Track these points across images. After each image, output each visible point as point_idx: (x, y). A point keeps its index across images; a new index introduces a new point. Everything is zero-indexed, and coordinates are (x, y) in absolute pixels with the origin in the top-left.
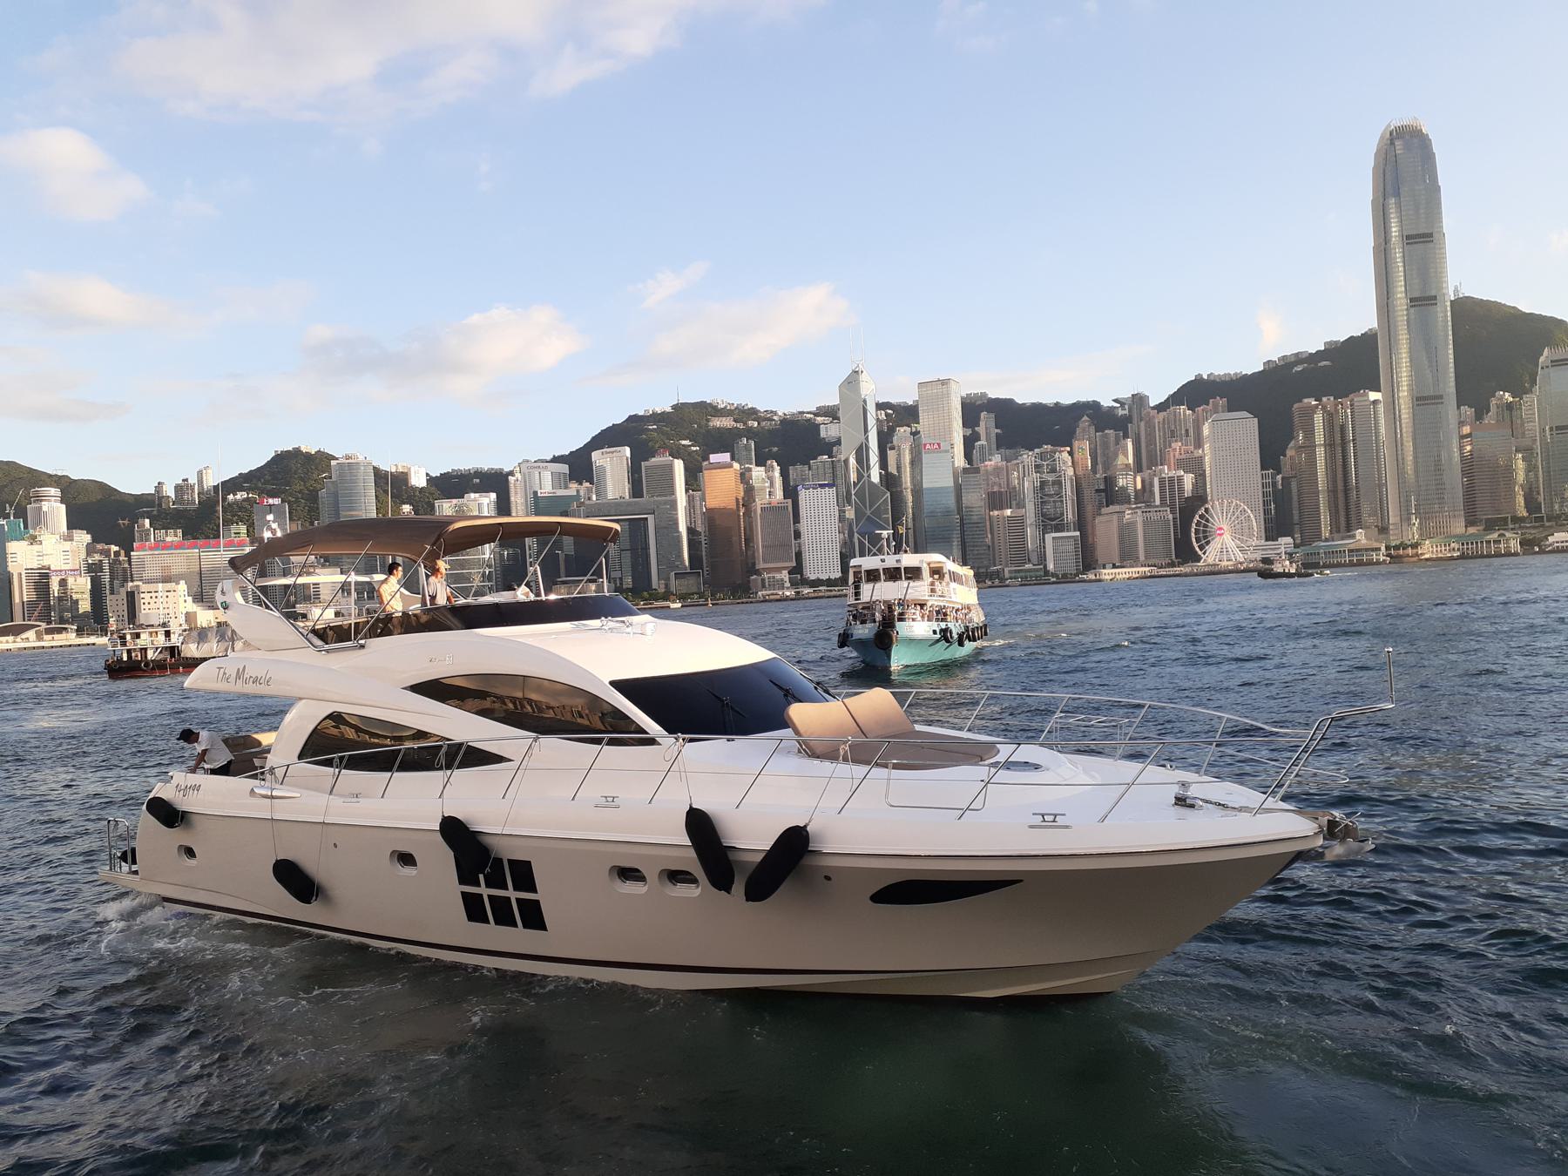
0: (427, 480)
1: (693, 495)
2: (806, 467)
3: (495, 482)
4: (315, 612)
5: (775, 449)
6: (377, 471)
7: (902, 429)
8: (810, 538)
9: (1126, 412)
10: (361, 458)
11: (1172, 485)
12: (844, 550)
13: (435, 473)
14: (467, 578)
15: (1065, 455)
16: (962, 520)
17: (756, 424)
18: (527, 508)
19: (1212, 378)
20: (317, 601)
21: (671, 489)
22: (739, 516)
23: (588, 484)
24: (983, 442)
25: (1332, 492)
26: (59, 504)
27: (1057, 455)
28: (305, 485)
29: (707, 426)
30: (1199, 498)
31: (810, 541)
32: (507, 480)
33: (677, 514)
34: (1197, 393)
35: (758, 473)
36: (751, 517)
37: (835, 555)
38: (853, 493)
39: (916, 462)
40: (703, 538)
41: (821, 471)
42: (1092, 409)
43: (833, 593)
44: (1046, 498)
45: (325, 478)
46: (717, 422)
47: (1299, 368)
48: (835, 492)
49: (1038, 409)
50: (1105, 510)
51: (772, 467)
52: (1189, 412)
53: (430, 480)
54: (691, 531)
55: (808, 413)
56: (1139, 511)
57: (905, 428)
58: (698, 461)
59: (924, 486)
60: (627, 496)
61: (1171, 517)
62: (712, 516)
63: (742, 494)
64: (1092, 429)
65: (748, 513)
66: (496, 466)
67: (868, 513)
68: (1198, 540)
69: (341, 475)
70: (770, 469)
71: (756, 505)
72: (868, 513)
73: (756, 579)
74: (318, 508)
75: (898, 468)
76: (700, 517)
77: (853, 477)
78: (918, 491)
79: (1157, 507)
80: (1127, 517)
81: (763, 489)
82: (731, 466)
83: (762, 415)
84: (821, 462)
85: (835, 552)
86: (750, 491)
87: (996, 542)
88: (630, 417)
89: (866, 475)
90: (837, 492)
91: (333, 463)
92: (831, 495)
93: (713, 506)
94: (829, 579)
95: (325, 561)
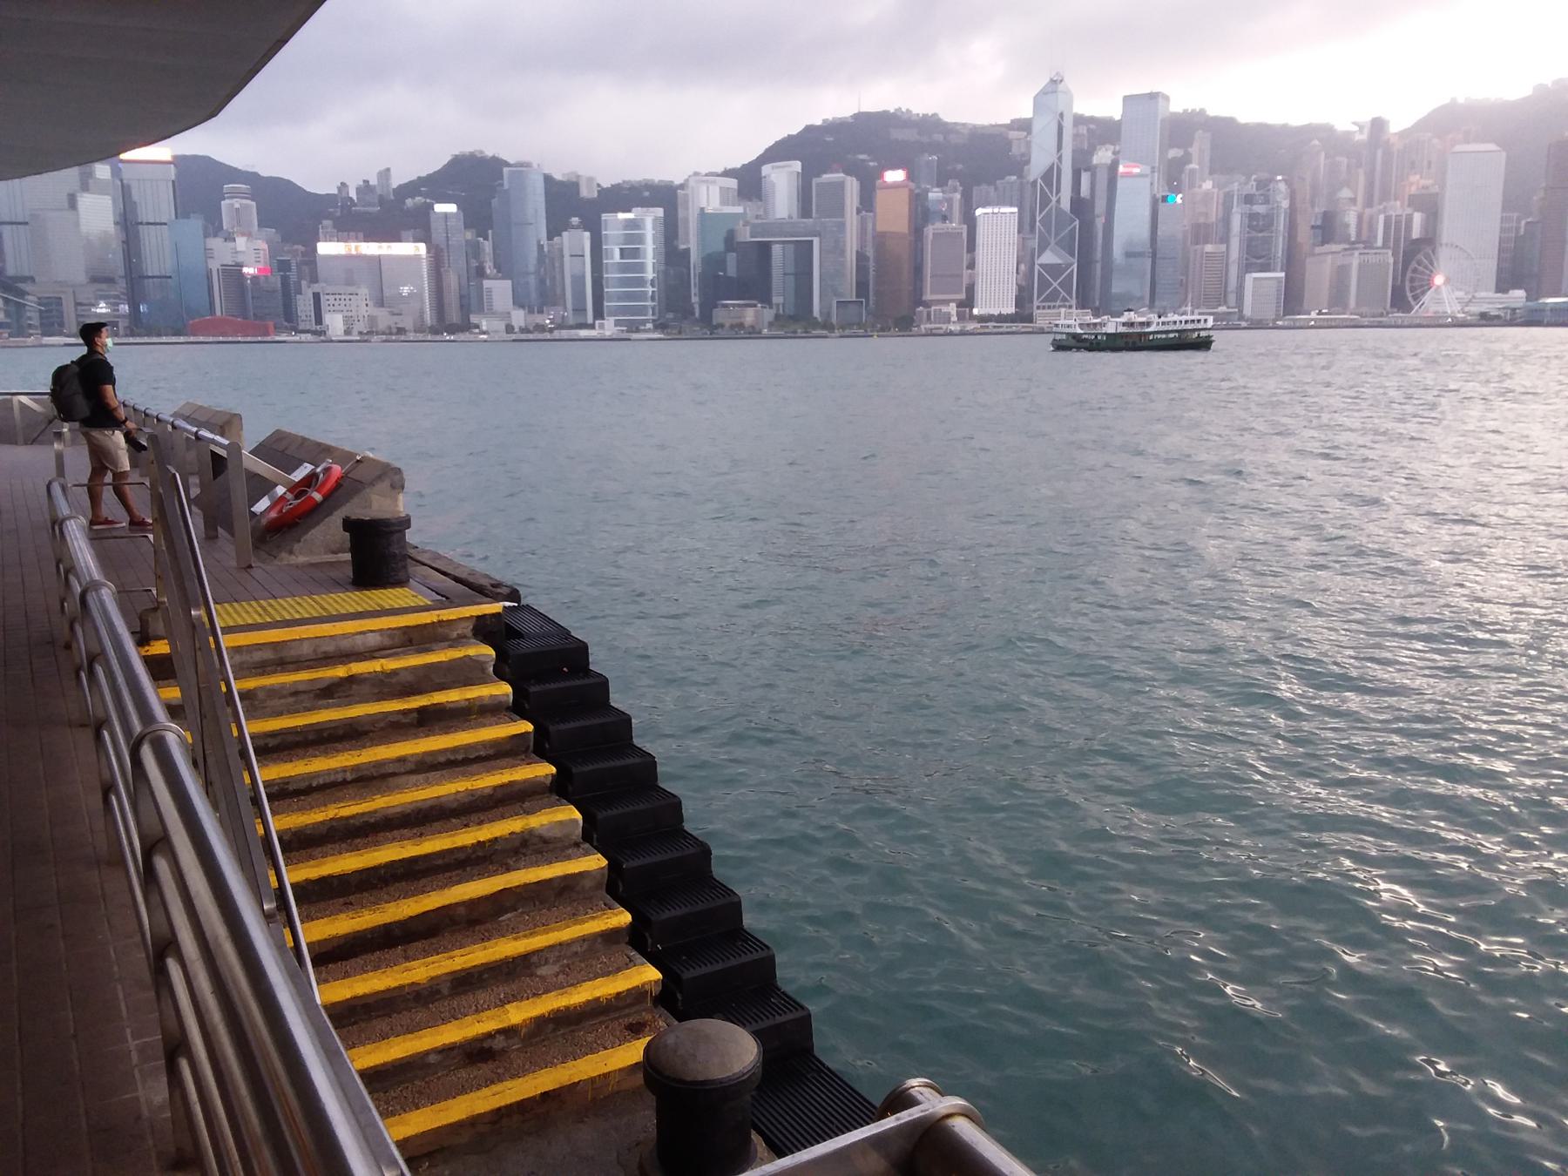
2: (992, 189)
3: (665, 196)
6: (548, 179)
12: (1019, 282)
21: (840, 210)
24: (1194, 166)
26: (249, 202)
27: (1271, 186)
30: (1429, 241)
38: (1038, 219)
43: (1001, 330)
50: (1318, 250)
54: (861, 257)
61: (1391, 260)
62: (881, 239)
68: (1413, 289)
73: (921, 312)
79: (1378, 248)
89: (1054, 199)
94: (1000, 315)
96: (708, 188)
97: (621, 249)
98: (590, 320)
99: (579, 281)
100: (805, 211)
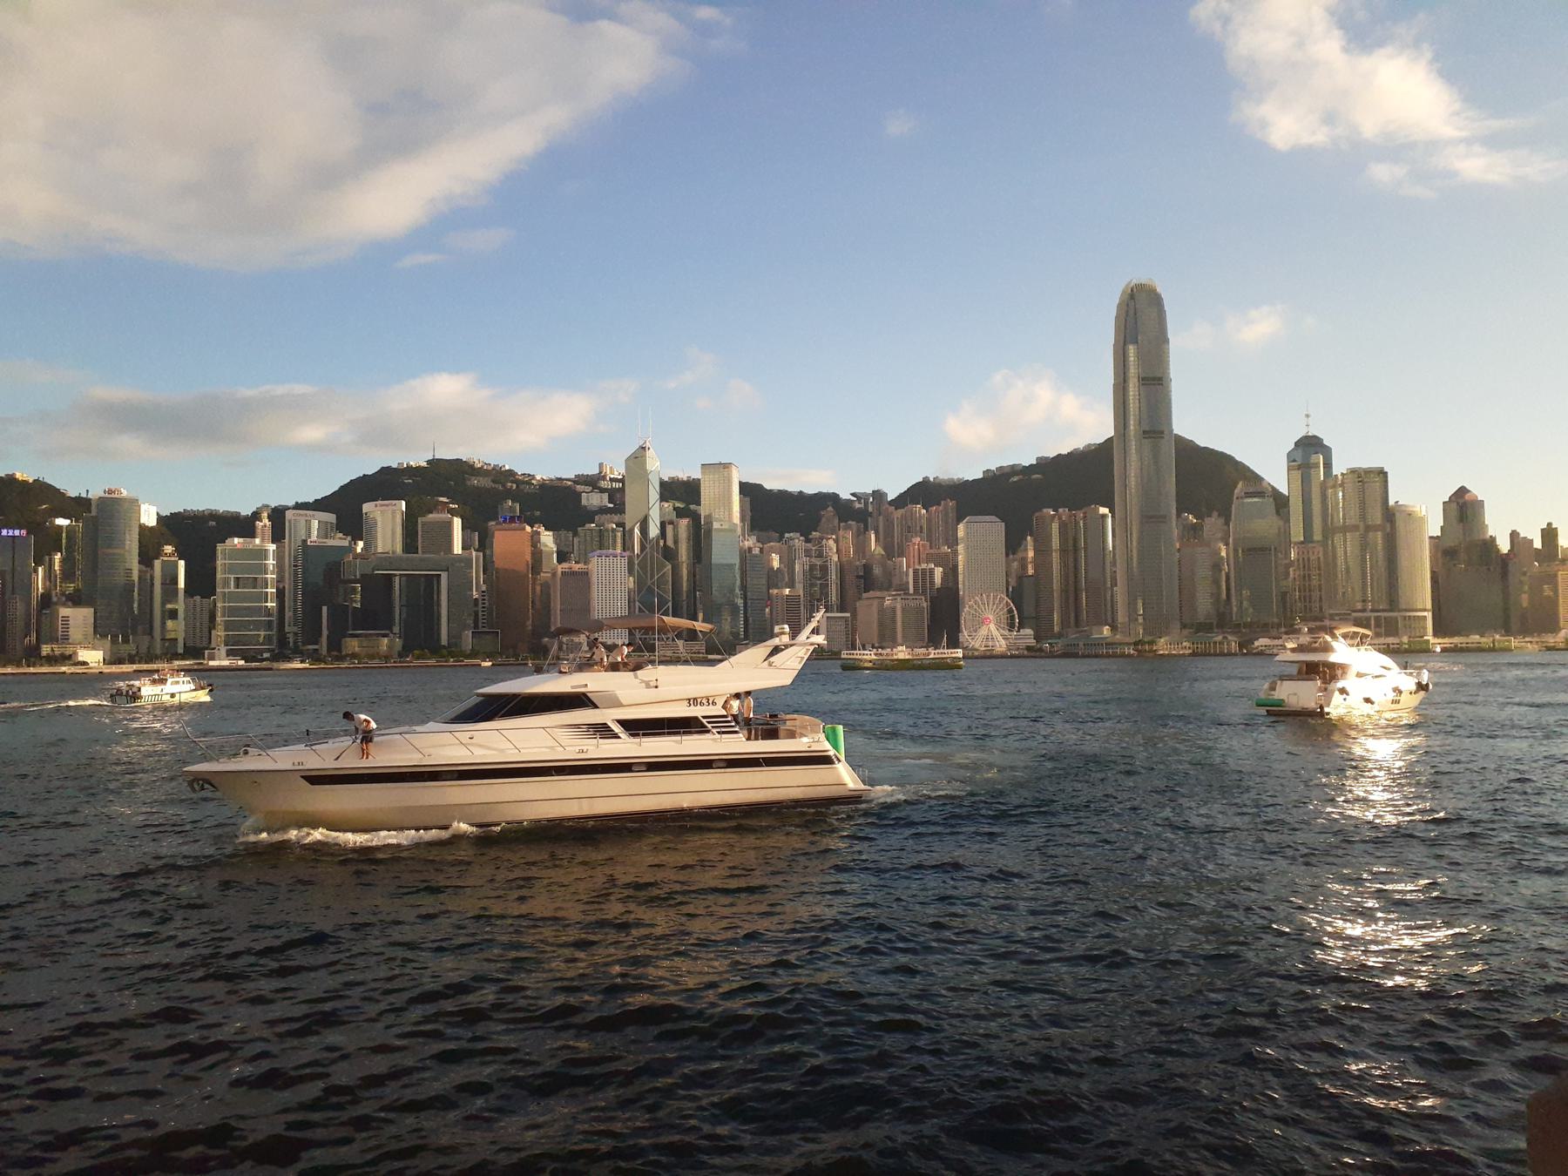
9: (862, 506)
11: (924, 577)
15: (831, 542)
19: (937, 481)
25: (1064, 591)
27: (824, 541)
34: (924, 492)
42: (833, 498)
44: (813, 581)
47: (1015, 479)
49: (783, 495)
50: (865, 595)
52: (924, 511)
56: (899, 598)
64: (836, 521)
80: (887, 602)
87: (774, 617)
100: (410, 543)
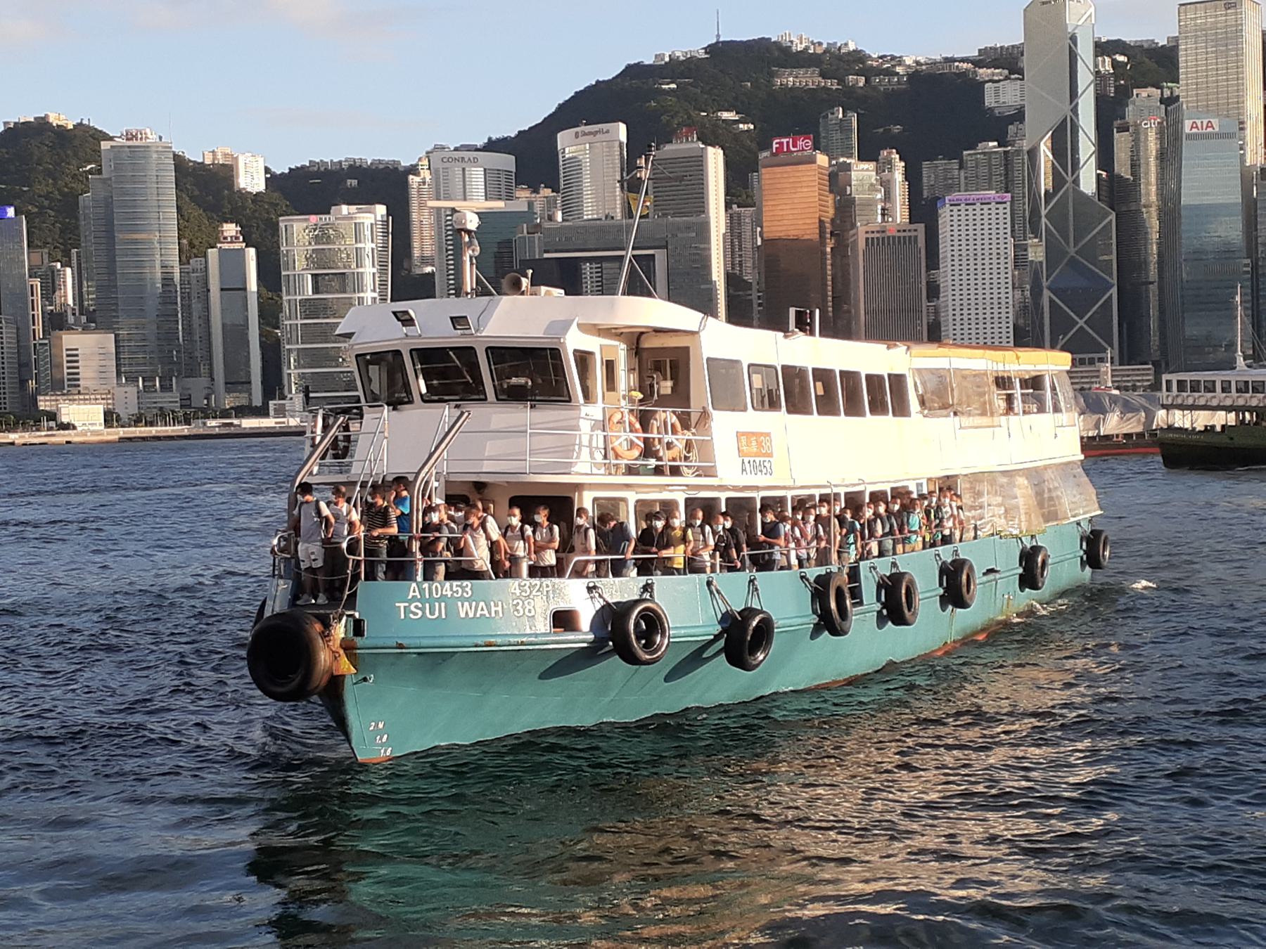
0: (266, 179)
1: (739, 215)
2: (955, 164)
4: (70, 411)
5: (897, 129)
6: (179, 161)
7: (1144, 93)
8: (957, 297)
10: (152, 138)
12: (1021, 322)
13: (281, 168)
14: (329, 357)
16: (1255, 267)
17: (862, 81)
18: (439, 234)
20: (74, 390)
21: (700, 204)
22: (824, 253)
23: (547, 192)
28: (55, 184)
29: (770, 83)
31: (958, 303)
32: (405, 186)
33: (709, 249)
35: (862, 173)
36: (846, 256)
37: (1004, 330)
38: (1043, 212)
39: (1170, 155)
40: (754, 294)
41: (983, 171)
45: (90, 172)
46: (790, 79)
48: (1008, 211)
51: (890, 162)
53: (273, 180)
55: (963, 60)
57: (1151, 90)
58: (749, 151)
59: (1184, 201)
60: (619, 216)
63: (831, 212)
65: (842, 248)
66: (387, 156)
67: (1072, 251)
69: (118, 167)
70: (884, 167)
71: (856, 234)
72: (1072, 251)
74: (77, 227)
75: (1132, 166)
76: (750, 254)
77: (1045, 182)
78: (1171, 211)
81: (870, 204)
82: (812, 160)
83: (875, 64)
84: (984, 154)
85: (1004, 325)
86: (846, 207)
88: (629, 67)
89: (1069, 179)
90: (1012, 210)
91: (105, 145)
92: (1001, 216)
93: (771, 236)
95: (89, 321)
96: (464, 169)
97: (314, 276)
98: (257, 401)
99: (235, 335)
